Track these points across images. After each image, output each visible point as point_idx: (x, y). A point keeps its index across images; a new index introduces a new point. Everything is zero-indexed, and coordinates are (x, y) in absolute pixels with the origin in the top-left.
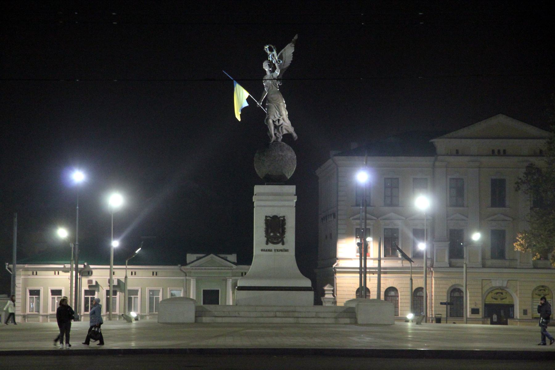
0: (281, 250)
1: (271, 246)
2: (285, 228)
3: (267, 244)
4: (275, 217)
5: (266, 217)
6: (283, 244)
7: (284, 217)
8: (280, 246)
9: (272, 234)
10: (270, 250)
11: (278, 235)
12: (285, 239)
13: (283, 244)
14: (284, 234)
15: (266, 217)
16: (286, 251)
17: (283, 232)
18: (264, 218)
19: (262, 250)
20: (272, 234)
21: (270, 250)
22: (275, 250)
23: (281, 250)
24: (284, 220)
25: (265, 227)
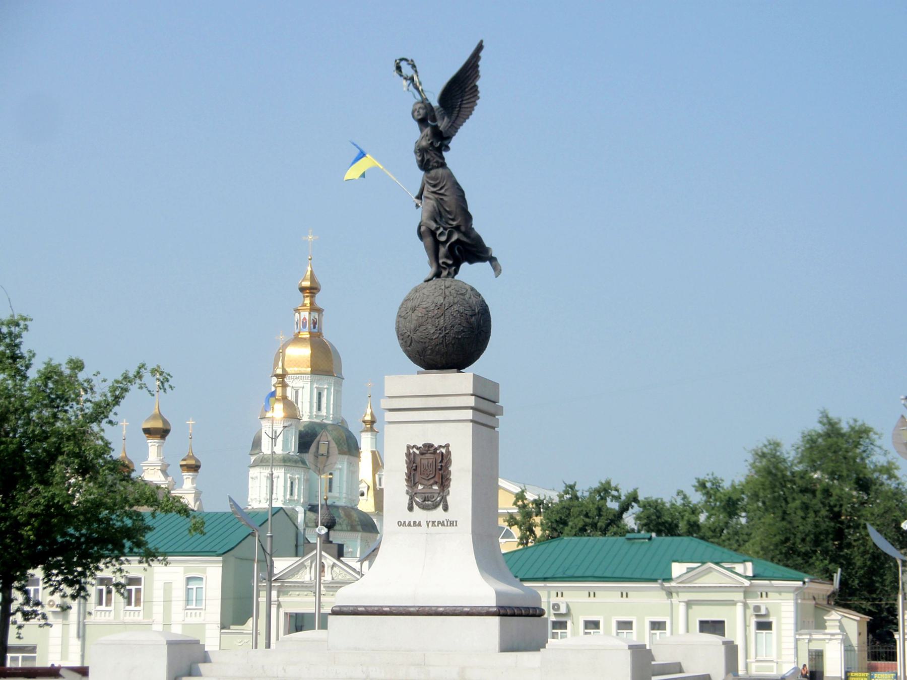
1: (419, 514)
2: (449, 473)
3: (411, 509)
4: (428, 446)
6: (446, 509)
7: (447, 446)
8: (438, 514)
9: (420, 487)
10: (417, 524)
13: (446, 509)
15: (408, 447)
16: (452, 524)
17: (444, 481)
19: (400, 524)
21: (417, 524)
24: (449, 453)
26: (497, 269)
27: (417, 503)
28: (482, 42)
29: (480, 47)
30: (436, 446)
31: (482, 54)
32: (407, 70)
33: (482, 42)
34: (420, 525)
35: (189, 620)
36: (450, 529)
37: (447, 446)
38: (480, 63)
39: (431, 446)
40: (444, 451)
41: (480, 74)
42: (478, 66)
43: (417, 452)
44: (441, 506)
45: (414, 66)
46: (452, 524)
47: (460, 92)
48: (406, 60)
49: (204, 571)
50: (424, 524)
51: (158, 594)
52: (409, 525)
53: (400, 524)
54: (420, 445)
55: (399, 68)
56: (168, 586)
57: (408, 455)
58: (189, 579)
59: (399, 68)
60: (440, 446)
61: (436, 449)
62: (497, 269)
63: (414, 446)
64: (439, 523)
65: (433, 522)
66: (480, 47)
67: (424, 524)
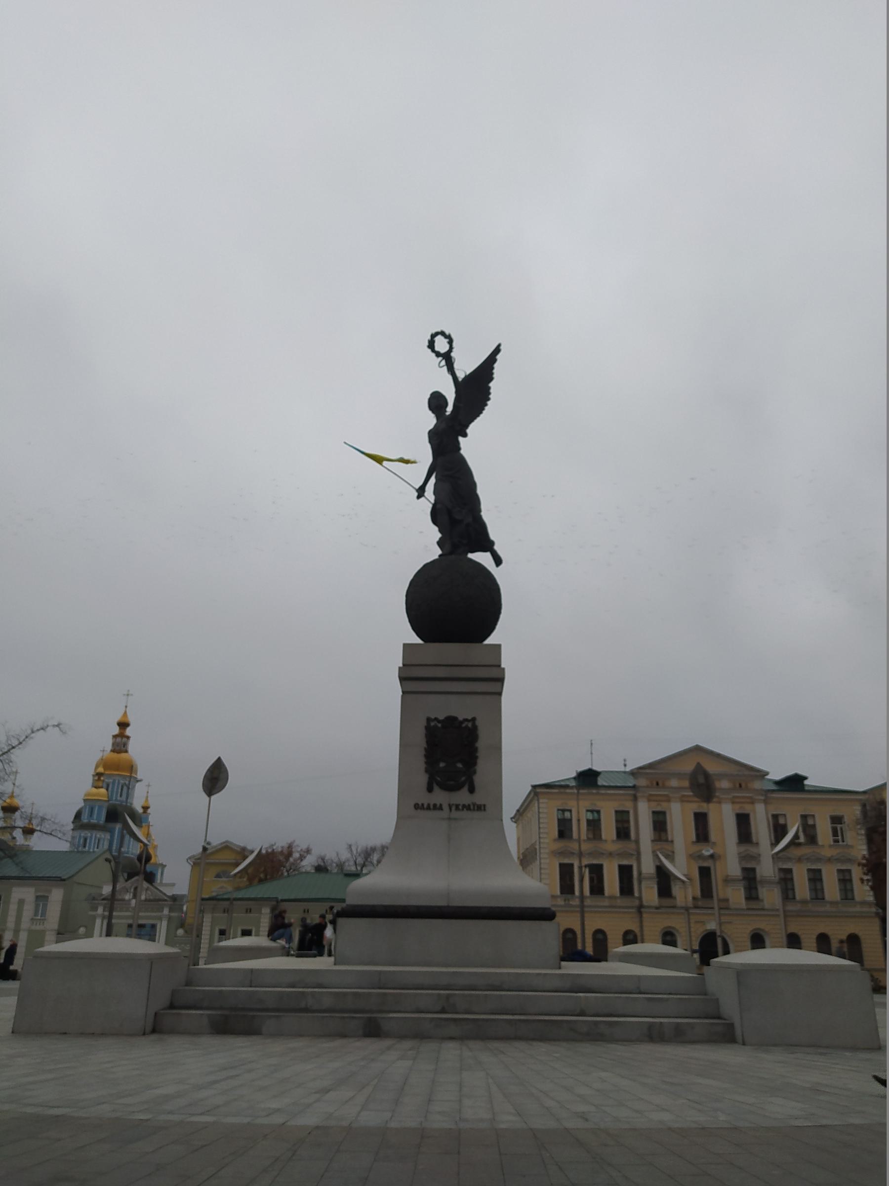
0: (467, 808)
1: (440, 796)
2: (476, 750)
3: (430, 789)
4: (451, 720)
5: (429, 720)
6: (472, 790)
7: (474, 719)
8: (462, 797)
9: (442, 765)
10: (438, 808)
11: (460, 765)
12: (477, 779)
14: (475, 764)
15: (429, 720)
16: (480, 808)
18: (424, 723)
19: (417, 807)
20: (442, 765)
21: (438, 808)
22: (450, 806)
23: (467, 808)
24: (475, 728)
25: (425, 745)
26: (498, 561)
27: (439, 784)
28: (499, 345)
29: (497, 350)
30: (461, 719)
31: (498, 357)
32: (441, 345)
33: (499, 345)
34: (441, 808)
35: (34, 927)
36: (477, 814)
37: (474, 719)
38: (496, 365)
39: (455, 718)
40: (470, 725)
41: (495, 376)
42: (493, 368)
43: (440, 725)
44: (465, 789)
45: (451, 342)
46: (480, 808)
47: (475, 391)
48: (442, 333)
49: (50, 891)
50: (446, 807)
51: (13, 908)
52: (428, 808)
53: (417, 807)
54: (441, 718)
55: (431, 345)
56: (21, 902)
57: (427, 728)
58: (37, 897)
59: (431, 345)
60: (466, 720)
61: (462, 722)
62: (498, 561)
63: (436, 719)
64: (464, 806)
65: (457, 807)
66: (497, 350)
67: (446, 807)
